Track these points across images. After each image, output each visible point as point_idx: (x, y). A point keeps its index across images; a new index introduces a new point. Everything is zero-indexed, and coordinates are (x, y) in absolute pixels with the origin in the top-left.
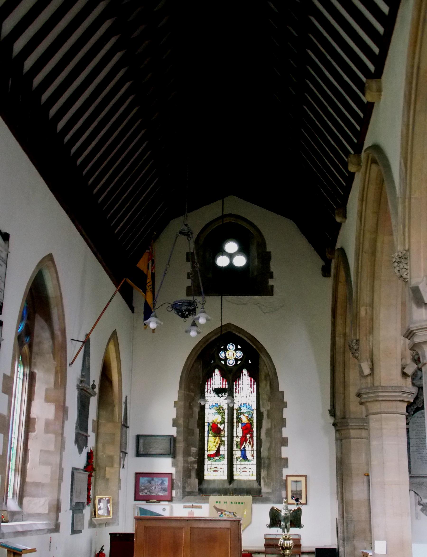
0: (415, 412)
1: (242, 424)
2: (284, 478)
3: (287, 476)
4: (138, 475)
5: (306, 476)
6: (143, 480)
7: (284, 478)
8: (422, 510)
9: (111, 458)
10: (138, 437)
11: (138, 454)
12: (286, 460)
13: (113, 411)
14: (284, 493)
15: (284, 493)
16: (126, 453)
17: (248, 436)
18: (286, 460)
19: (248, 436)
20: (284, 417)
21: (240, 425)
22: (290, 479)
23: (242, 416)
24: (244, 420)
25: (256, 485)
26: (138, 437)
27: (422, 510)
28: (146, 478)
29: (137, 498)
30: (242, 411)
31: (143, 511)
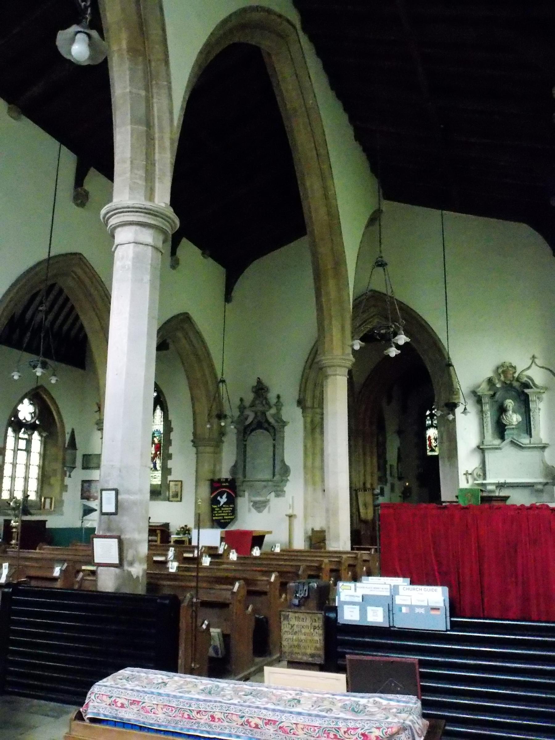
0: (251, 432)
1: (155, 444)
2: (168, 482)
3: (170, 481)
4: (84, 482)
5: (181, 481)
6: (86, 485)
7: (168, 482)
8: (253, 506)
9: (55, 471)
10: (84, 456)
11: (84, 468)
12: (170, 469)
13: (57, 440)
14: (167, 493)
15: (167, 493)
16: (74, 468)
17: (158, 453)
18: (170, 469)
19: (158, 453)
20: (171, 438)
21: (154, 446)
22: (172, 484)
23: (155, 439)
24: (156, 441)
25: (159, 489)
26: (84, 456)
27: (253, 506)
28: (87, 484)
29: (83, 498)
30: (155, 435)
31: (84, 505)
